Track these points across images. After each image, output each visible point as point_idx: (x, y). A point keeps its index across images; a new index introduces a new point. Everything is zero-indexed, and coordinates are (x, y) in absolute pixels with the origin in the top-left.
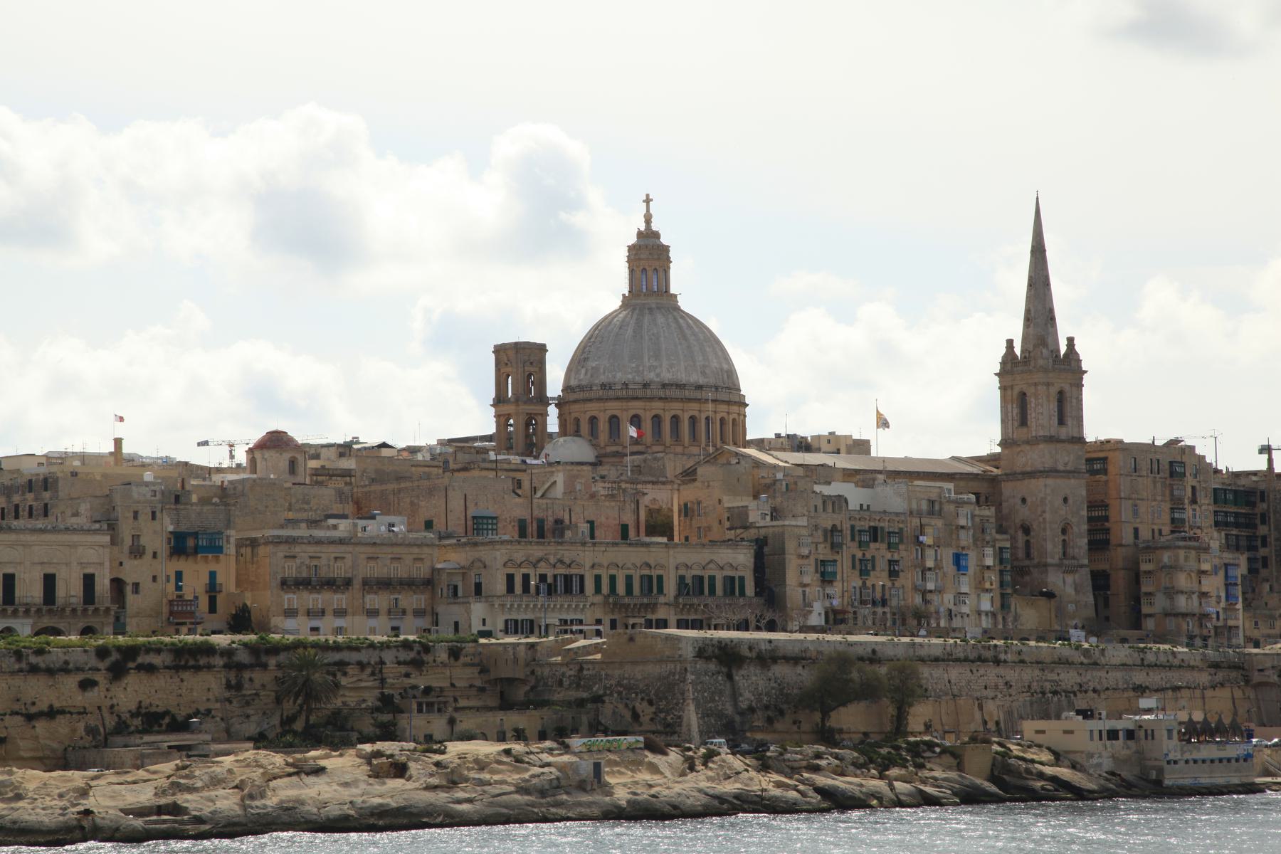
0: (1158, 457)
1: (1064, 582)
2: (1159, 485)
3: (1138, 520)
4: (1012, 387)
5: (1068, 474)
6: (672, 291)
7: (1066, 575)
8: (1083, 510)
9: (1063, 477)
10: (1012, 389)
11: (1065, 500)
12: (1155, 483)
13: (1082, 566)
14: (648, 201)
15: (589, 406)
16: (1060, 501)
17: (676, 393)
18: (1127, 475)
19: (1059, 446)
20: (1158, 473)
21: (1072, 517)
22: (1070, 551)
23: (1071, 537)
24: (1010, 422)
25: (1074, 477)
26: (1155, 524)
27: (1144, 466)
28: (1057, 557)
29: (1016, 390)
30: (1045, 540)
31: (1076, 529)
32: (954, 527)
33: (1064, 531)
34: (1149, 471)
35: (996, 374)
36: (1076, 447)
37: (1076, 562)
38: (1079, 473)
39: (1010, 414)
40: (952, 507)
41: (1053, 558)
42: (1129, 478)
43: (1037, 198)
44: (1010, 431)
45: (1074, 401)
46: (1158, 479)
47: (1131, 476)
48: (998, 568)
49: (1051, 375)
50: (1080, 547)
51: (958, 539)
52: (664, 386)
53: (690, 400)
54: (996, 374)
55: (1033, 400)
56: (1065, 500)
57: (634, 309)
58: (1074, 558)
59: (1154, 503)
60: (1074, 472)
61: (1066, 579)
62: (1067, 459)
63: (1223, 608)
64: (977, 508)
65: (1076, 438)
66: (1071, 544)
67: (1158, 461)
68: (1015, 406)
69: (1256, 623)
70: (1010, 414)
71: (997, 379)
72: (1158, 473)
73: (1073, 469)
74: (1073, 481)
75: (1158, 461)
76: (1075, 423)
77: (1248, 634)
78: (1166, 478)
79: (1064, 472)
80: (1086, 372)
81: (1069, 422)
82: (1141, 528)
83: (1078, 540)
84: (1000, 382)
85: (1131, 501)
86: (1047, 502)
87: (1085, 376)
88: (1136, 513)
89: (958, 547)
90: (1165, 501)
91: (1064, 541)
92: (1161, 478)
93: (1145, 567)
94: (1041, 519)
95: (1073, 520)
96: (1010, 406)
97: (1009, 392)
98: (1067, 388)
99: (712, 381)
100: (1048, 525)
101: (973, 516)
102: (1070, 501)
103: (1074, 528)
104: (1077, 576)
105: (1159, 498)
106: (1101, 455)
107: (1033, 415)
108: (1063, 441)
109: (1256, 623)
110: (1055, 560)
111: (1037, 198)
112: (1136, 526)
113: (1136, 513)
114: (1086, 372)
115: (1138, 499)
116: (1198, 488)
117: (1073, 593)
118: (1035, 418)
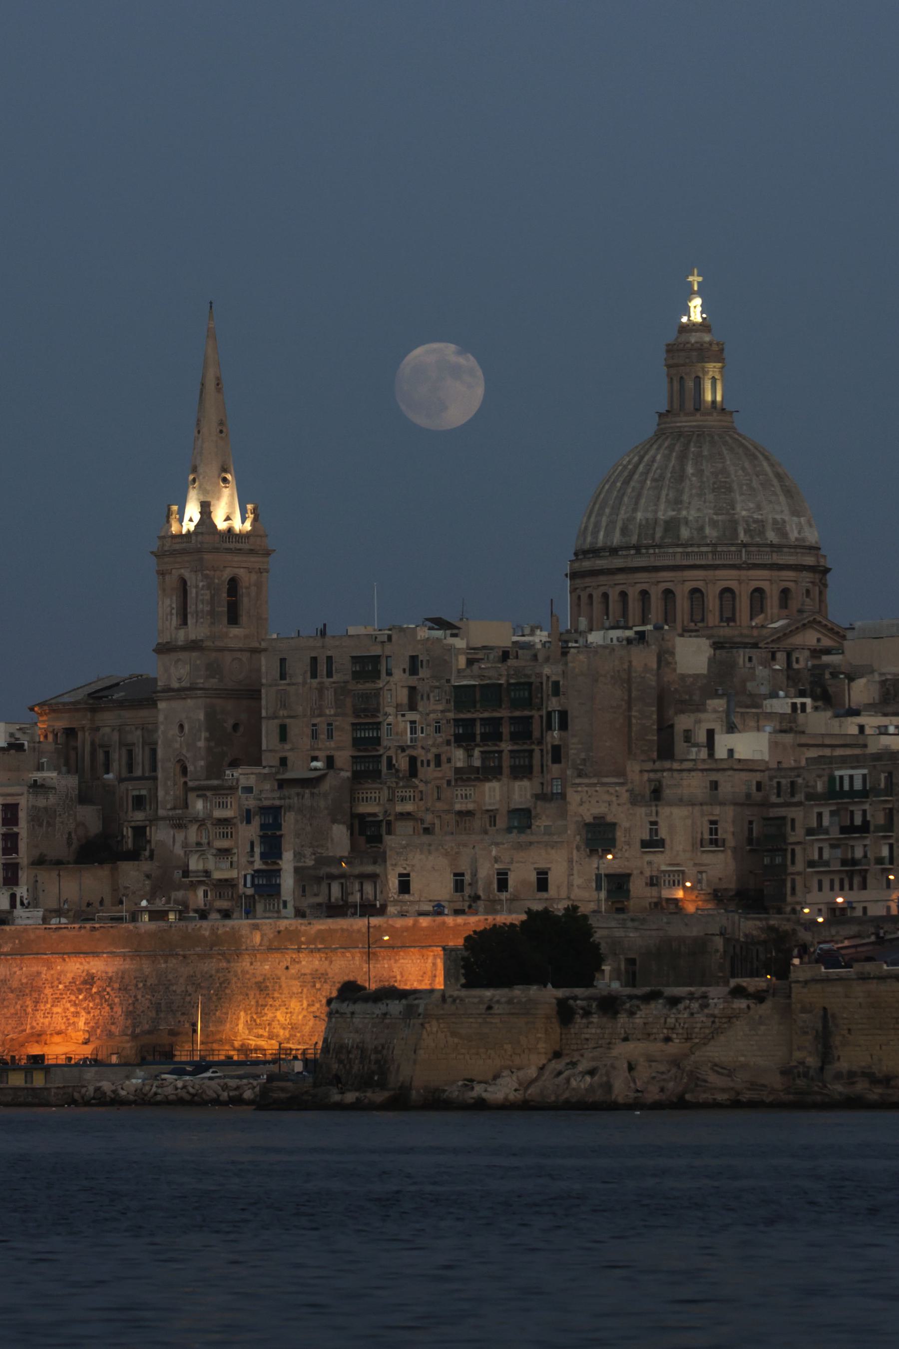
0: (329, 653)
2: (329, 695)
3: (287, 747)
8: (200, 740)
11: (181, 727)
16: (176, 730)
20: (329, 674)
26: (320, 749)
27: (299, 668)
36: (194, 654)
56: (181, 727)
61: (176, 834)
72: (329, 674)
73: (188, 685)
75: (330, 659)
92: (334, 683)
95: (188, 755)
99: (634, 540)
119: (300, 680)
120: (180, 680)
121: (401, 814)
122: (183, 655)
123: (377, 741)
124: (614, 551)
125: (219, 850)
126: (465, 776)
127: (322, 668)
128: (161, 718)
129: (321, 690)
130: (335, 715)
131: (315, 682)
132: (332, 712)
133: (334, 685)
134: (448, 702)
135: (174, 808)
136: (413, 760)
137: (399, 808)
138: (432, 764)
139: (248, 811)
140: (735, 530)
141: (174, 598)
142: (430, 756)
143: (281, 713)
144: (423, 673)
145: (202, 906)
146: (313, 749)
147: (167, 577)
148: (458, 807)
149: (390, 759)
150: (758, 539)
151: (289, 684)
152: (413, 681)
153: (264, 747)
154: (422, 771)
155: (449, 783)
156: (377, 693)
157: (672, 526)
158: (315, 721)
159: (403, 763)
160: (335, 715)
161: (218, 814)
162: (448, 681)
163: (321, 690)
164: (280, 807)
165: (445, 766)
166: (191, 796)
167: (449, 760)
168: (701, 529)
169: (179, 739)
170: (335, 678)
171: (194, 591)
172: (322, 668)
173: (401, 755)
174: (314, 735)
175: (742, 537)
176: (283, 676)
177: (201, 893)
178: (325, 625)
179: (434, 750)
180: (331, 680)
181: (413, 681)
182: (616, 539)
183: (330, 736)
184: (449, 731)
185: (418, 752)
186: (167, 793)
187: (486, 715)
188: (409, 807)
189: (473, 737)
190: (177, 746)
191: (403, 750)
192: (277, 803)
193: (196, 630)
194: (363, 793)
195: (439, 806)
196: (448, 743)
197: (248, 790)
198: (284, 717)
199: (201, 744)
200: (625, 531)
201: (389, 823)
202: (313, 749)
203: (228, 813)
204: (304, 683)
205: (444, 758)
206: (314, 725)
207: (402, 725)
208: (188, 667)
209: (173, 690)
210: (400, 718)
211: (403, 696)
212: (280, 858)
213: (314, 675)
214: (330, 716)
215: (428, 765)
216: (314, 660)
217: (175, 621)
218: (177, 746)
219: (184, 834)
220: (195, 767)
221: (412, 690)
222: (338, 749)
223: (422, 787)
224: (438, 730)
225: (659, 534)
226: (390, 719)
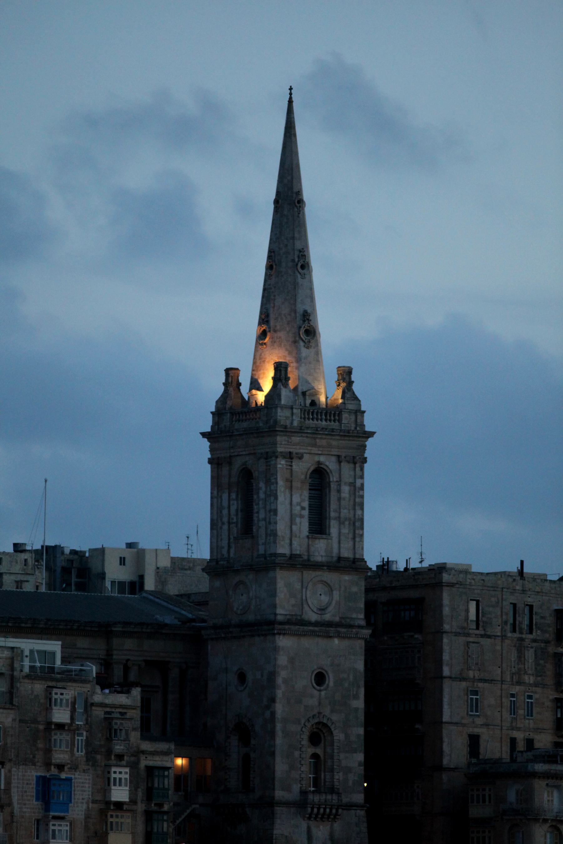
0: (529, 600)
2: (530, 655)
3: (479, 721)
4: (230, 461)
7: (312, 823)
8: (356, 697)
9: (313, 634)
10: (230, 463)
12: (520, 648)
13: (350, 806)
18: (457, 634)
19: (309, 575)
21: (332, 711)
23: (329, 750)
24: (226, 527)
25: (339, 636)
26: (518, 729)
28: (296, 788)
29: (238, 463)
30: (273, 754)
31: (339, 735)
32: (41, 727)
33: (315, 739)
34: (508, 627)
35: (204, 435)
37: (335, 797)
38: (351, 626)
39: (225, 512)
40: (39, 687)
42: (462, 639)
43: (290, 102)
44: (225, 543)
45: (346, 489)
46: (527, 642)
47: (468, 635)
48: (141, 807)
49: (296, 439)
50: (348, 770)
51: (48, 751)
54: (204, 435)
55: (262, 485)
56: (320, 678)
57: (355, 463)
58: (332, 790)
59: (516, 689)
61: (314, 830)
62: (325, 599)
64: (98, 689)
65: (346, 559)
66: (329, 763)
67: (531, 607)
68: (233, 496)
70: (225, 512)
71: (206, 444)
74: (336, 641)
76: (345, 531)
78: (547, 642)
80: (371, 434)
82: (485, 734)
83: (342, 756)
84: (212, 450)
85: (464, 684)
86: (279, 681)
87: (370, 443)
88: (475, 706)
89: (48, 764)
90: (544, 686)
91: (315, 756)
92: (535, 641)
93: (476, 811)
94: (268, 714)
95: (335, 717)
96: (225, 496)
97: (225, 470)
100: (279, 726)
101: (89, 705)
102: (331, 681)
103: (335, 732)
104: (337, 826)
105: (529, 679)
106: (414, 594)
107: (262, 516)
108: (317, 566)
110: (294, 794)
111: (290, 102)
112: (476, 731)
113: (475, 706)
114: (371, 434)
115: (485, 681)
118: (265, 519)
128: (282, 660)
130: (536, 685)
132: (532, 680)
133: (534, 644)
143: (471, 674)
146: (512, 729)
151: (482, 636)
153: (446, 717)
160: (536, 685)
166: (539, 785)
169: (316, 693)
174: (513, 710)
178: (522, 562)
180: (531, 636)
194: (89, 779)
198: (474, 680)
199: (359, 704)
206: (513, 695)
214: (530, 685)
218: (313, 702)
219: (328, 827)
220: (347, 736)
222: (537, 730)
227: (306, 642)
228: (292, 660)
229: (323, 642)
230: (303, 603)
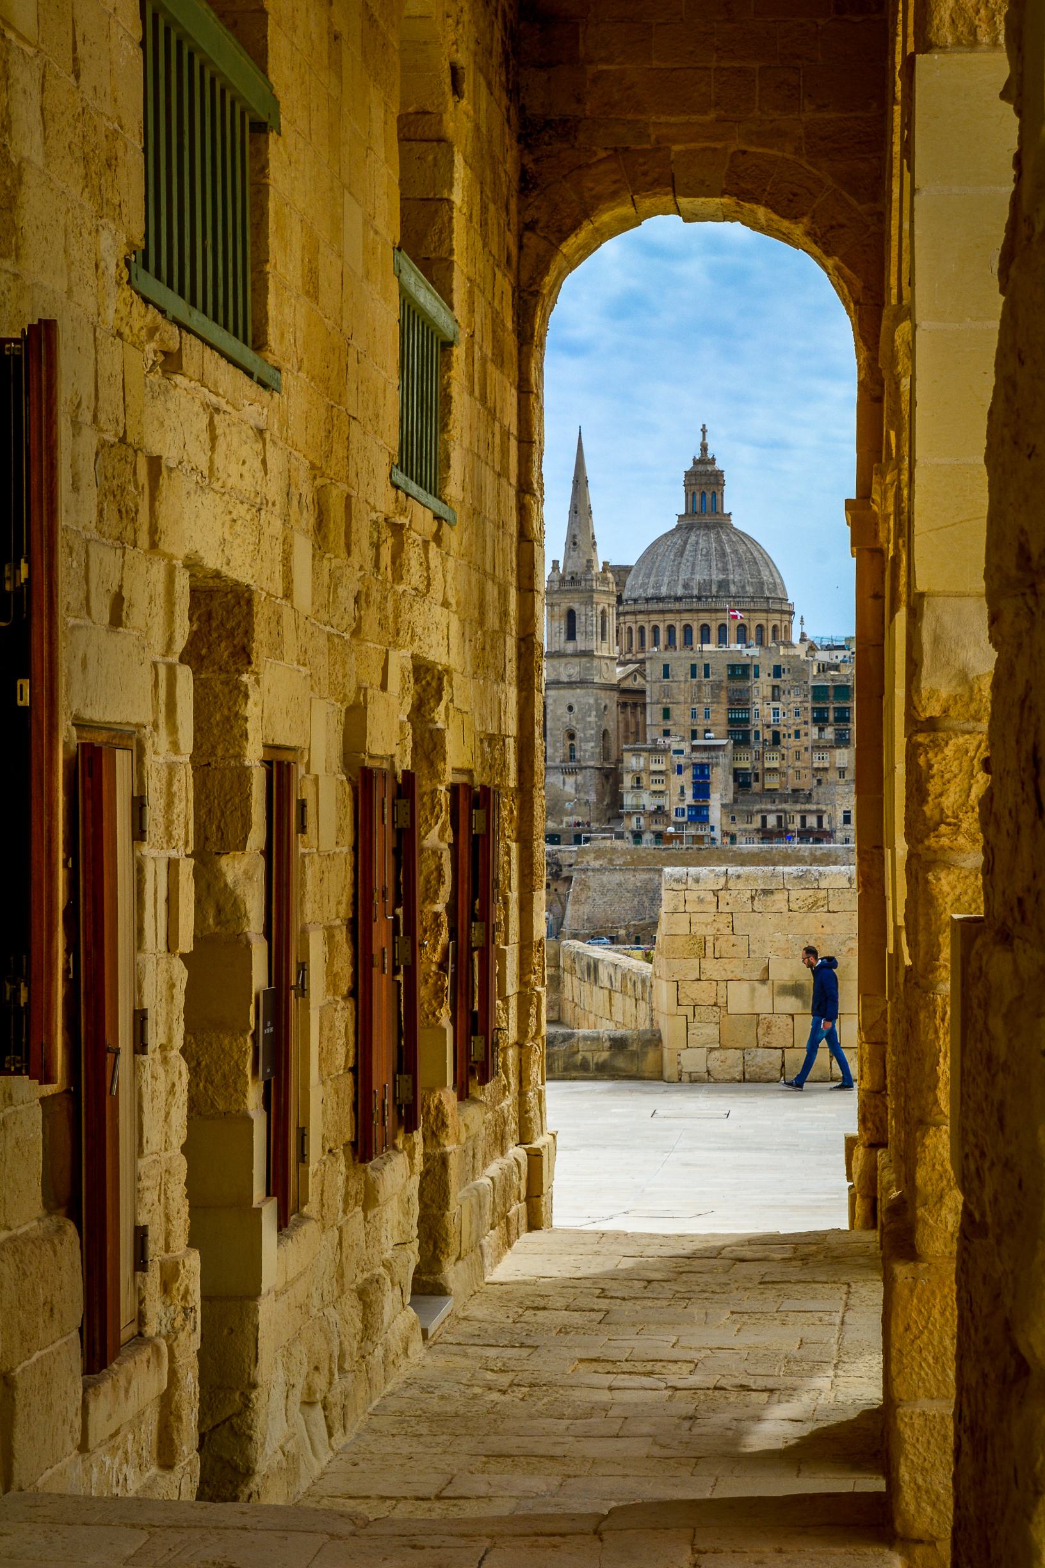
1: (564, 783)
2: (707, 690)
3: (670, 723)
5: (571, 685)
6: (726, 511)
11: (570, 708)
14: (704, 431)
15: (702, 615)
17: (653, 606)
19: (564, 661)
20: (707, 675)
22: (578, 754)
25: (581, 688)
41: (554, 761)
42: (658, 684)
50: (586, 751)
52: (647, 600)
53: (663, 612)
56: (570, 708)
60: (580, 682)
63: (689, 806)
69: (733, 819)
72: (707, 675)
75: (707, 667)
77: (725, 828)
79: (568, 683)
81: (578, 636)
98: (576, 606)
99: (695, 592)
102: (576, 709)
104: (579, 777)
109: (733, 819)
116: (782, 686)
117: (573, 791)
119: (682, 679)
120: (570, 676)
121: (768, 769)
122: (577, 660)
123: (747, 721)
124: (678, 599)
125: (655, 792)
126: (817, 747)
127: (701, 672)
129: (699, 686)
131: (694, 681)
134: (806, 696)
135: (563, 761)
136: (776, 735)
137: (767, 765)
138: (793, 737)
139: (679, 767)
140: (762, 589)
141: (563, 622)
142: (791, 731)
144: (784, 677)
145: (635, 828)
147: (556, 609)
148: (816, 765)
149: (757, 733)
150: (773, 595)
152: (777, 682)
154: (784, 742)
155: (806, 749)
156: (748, 690)
157: (723, 585)
158: (694, 706)
159: (768, 735)
161: (654, 767)
162: (806, 682)
163: (699, 686)
164: (708, 765)
165: (803, 738)
167: (806, 734)
168: (743, 587)
170: (711, 678)
171: (583, 618)
172: (701, 672)
173: (766, 730)
174: (694, 715)
175: (767, 594)
176: (666, 675)
177: (634, 819)
179: (794, 728)
181: (777, 682)
182: (680, 592)
183: (707, 716)
184: (809, 716)
185: (783, 730)
186: (556, 750)
187: (837, 705)
188: (775, 764)
189: (826, 720)
190: (564, 720)
191: (768, 726)
192: (706, 761)
193: (581, 644)
195: (798, 764)
196: (806, 723)
197: (680, 752)
200: (686, 586)
201: (757, 775)
202: (693, 725)
203: (662, 767)
204: (686, 681)
205: (802, 733)
207: (766, 712)
208: (577, 669)
209: (563, 683)
210: (765, 706)
211: (768, 692)
212: (708, 797)
213: (694, 675)
215: (789, 736)
216: (693, 667)
217: (563, 637)
221: (774, 687)
223: (784, 751)
224: (797, 714)
225: (714, 589)
226: (757, 707)
227: (562, 692)
228: (555, 701)
229: (572, 692)
230: (559, 674)
